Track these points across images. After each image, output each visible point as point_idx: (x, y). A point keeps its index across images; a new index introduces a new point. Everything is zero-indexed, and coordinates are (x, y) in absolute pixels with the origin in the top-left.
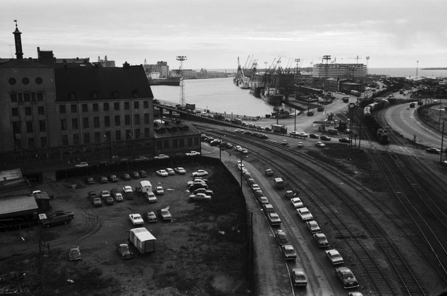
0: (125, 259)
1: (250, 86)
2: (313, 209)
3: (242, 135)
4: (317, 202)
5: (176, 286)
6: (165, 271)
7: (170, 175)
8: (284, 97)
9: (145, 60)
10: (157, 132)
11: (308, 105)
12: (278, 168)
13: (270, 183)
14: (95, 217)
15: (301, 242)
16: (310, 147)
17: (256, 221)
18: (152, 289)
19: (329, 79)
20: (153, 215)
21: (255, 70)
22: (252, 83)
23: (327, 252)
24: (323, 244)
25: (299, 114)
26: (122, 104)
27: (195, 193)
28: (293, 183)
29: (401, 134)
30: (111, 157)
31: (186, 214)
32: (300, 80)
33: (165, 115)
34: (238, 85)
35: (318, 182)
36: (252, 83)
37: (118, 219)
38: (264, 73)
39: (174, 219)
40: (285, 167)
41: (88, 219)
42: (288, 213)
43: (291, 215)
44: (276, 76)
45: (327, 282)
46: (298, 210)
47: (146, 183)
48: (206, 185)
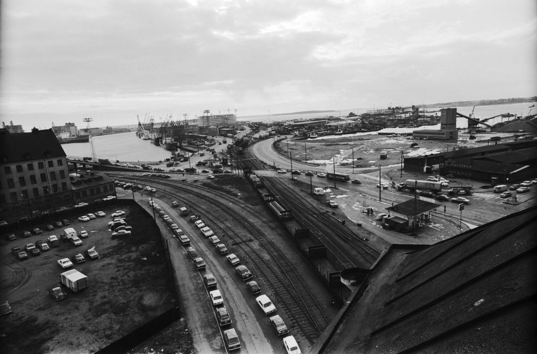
0: (60, 301)
1: (150, 137)
2: (213, 227)
3: (149, 177)
4: (215, 221)
5: (112, 311)
6: (100, 301)
7: (91, 219)
8: (178, 144)
9: (53, 122)
10: (74, 184)
11: (198, 148)
12: (181, 199)
13: (177, 212)
14: (23, 270)
15: (207, 253)
16: (204, 180)
17: (170, 244)
18: (90, 320)
19: (210, 127)
20: (81, 257)
21: (152, 124)
22: (152, 135)
23: (228, 257)
24: (224, 252)
25: (191, 156)
26: (36, 164)
27: (117, 231)
28: (195, 209)
29: (265, 162)
30: (31, 213)
31: (111, 250)
32: (189, 130)
33: (80, 168)
34: (140, 137)
35: (213, 205)
36: (152, 135)
37: (47, 266)
38: (160, 126)
39: (101, 256)
40: (186, 198)
41: (14, 273)
42: (194, 233)
43: (196, 234)
44: (170, 128)
45: (231, 279)
46: (201, 229)
47: (70, 231)
48: (125, 222)
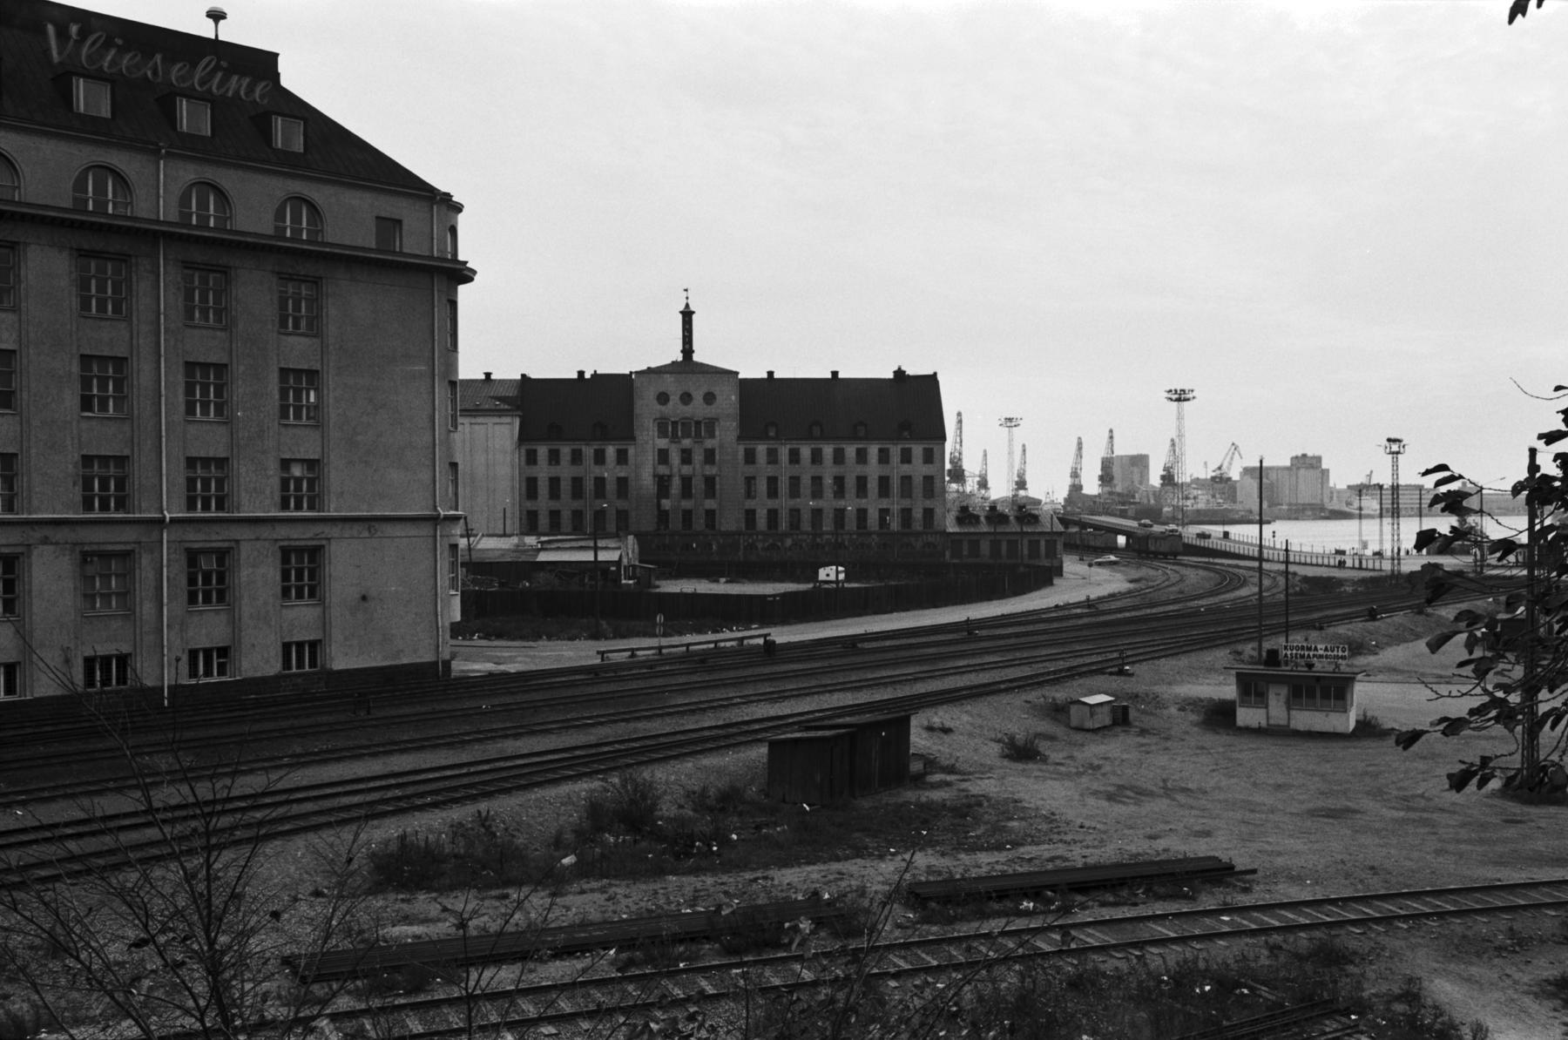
26: (873, 450)
